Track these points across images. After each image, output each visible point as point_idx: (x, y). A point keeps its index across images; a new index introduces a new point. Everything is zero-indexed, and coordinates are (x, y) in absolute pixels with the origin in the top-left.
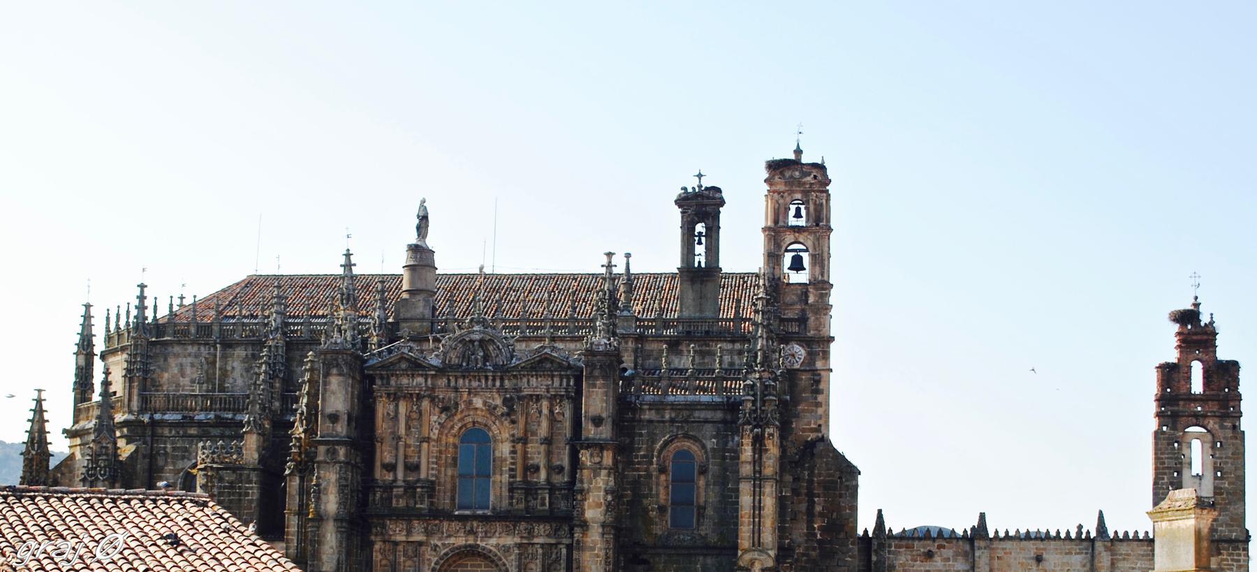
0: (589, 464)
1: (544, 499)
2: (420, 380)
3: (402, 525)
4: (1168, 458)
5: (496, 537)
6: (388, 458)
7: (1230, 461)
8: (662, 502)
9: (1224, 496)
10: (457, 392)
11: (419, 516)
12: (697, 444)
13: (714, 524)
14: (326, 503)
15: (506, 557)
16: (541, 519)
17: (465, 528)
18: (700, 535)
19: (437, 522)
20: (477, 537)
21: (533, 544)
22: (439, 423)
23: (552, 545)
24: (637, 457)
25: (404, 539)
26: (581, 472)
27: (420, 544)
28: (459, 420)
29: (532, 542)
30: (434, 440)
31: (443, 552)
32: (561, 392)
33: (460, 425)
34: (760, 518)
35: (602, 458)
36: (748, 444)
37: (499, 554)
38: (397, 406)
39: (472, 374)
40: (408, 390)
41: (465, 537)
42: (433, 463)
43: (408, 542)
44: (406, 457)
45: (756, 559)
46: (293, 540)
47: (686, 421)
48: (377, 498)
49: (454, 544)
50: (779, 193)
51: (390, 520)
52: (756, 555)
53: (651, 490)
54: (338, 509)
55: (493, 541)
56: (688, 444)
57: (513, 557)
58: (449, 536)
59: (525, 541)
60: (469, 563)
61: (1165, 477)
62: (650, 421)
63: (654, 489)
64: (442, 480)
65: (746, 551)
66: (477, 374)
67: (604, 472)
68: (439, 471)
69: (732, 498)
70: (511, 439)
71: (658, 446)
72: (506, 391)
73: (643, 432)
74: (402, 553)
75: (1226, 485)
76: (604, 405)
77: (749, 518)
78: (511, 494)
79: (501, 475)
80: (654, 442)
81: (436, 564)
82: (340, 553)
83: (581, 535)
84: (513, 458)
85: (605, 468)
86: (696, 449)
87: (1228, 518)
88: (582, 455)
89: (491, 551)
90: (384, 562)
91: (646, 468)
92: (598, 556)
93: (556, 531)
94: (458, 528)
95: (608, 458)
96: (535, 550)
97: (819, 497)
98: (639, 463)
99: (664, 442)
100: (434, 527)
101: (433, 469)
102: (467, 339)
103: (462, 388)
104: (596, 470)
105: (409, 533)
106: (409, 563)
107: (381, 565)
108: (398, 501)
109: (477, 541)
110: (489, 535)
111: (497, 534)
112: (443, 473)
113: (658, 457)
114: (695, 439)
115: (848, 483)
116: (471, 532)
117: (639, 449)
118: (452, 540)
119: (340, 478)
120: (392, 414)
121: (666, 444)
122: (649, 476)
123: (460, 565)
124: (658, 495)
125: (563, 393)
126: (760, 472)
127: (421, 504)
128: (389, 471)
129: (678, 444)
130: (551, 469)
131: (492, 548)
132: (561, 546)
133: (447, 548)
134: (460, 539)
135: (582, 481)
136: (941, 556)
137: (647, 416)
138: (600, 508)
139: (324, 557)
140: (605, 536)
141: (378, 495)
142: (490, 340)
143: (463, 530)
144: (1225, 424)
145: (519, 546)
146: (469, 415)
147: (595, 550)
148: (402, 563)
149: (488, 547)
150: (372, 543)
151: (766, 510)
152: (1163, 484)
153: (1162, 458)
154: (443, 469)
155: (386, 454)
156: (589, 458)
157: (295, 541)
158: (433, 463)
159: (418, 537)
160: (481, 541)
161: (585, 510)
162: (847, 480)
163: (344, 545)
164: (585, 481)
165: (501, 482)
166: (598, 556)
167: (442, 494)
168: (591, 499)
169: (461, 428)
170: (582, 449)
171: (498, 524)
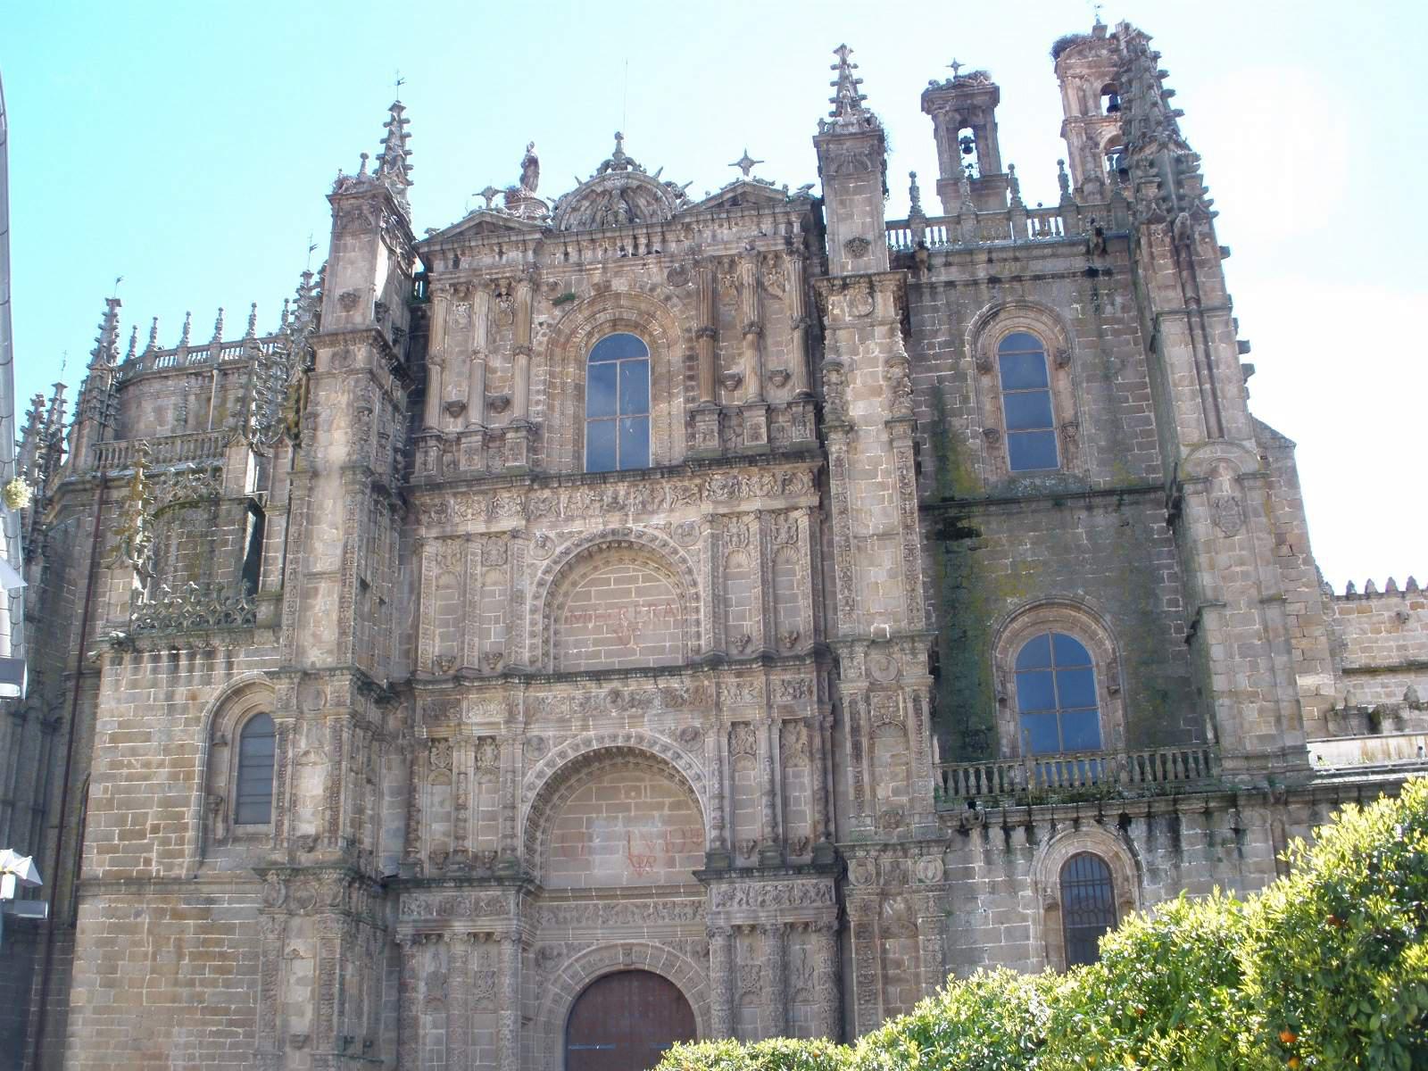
0: (848, 319)
1: (758, 426)
2: (514, 255)
3: (480, 503)
6: (453, 395)
8: (990, 423)
10: (581, 271)
11: (510, 479)
12: (1044, 318)
13: (1101, 450)
14: (326, 447)
15: (685, 547)
16: (751, 460)
17: (602, 500)
18: (1075, 477)
19: (547, 493)
20: (627, 515)
21: (739, 515)
22: (549, 326)
23: (776, 512)
24: (932, 346)
25: (482, 528)
26: (834, 334)
27: (515, 534)
28: (587, 319)
29: (738, 509)
30: (539, 354)
31: (558, 550)
32: (776, 245)
33: (588, 328)
34: (1213, 384)
35: (874, 305)
36: (1164, 257)
37: (672, 543)
38: (471, 306)
39: (609, 234)
40: (491, 274)
41: (604, 516)
42: (538, 392)
43: (489, 535)
44: (486, 388)
45: (1220, 460)
46: (276, 558)
47: (1018, 279)
48: (430, 460)
49: (581, 532)
50: (1081, 78)
51: (455, 495)
52: (1217, 451)
53: (966, 399)
54: (349, 454)
55: (659, 519)
56: (1028, 321)
57: (700, 545)
58: (570, 519)
59: (722, 510)
60: (612, 576)
62: (950, 284)
63: (972, 395)
64: (556, 422)
65: (1195, 447)
66: (617, 234)
67: (880, 331)
68: (551, 408)
69: (1127, 400)
70: (687, 335)
71: (970, 325)
72: (672, 257)
73: (939, 303)
74: (479, 558)
76: (868, 220)
77: (1192, 384)
78: (690, 430)
81: (546, 572)
82: (348, 533)
83: (844, 448)
84: (690, 368)
85: (882, 323)
86: (1043, 327)
88: (833, 305)
89: (654, 539)
90: (443, 580)
91: (952, 364)
92: (883, 486)
93: (786, 482)
94: (588, 502)
95: (885, 306)
96: (743, 528)
98: (935, 357)
99: (980, 317)
100: (542, 506)
101: (538, 402)
102: (599, 190)
103: (591, 264)
104: (866, 323)
105: (491, 515)
106: (494, 576)
108: (470, 460)
109: (626, 521)
110: (649, 508)
112: (557, 410)
113: (974, 342)
114: (1039, 308)
115: (1279, 465)
116: (616, 505)
117: (935, 333)
118: (577, 526)
119: (357, 399)
120: (463, 321)
121: (984, 323)
122: (960, 376)
123: (593, 582)
124: (980, 409)
125: (780, 247)
126: (1198, 301)
127: (516, 460)
128: (455, 415)
129: (1008, 322)
130: (765, 378)
131: (656, 533)
132: (795, 514)
134: (593, 520)
135: (837, 351)
136: (1419, 620)
137: (942, 276)
138: (880, 395)
139: (319, 546)
140: (895, 444)
141: (433, 453)
142: (638, 187)
143: (597, 505)
145: (713, 519)
146: (605, 309)
147: (876, 477)
148: (479, 577)
149: (649, 531)
150: (419, 545)
151: (1222, 367)
154: (557, 403)
155: (450, 388)
156: (846, 309)
157: (280, 560)
158: (538, 392)
159: (507, 523)
160: (635, 521)
161: (847, 402)
162: (1277, 460)
163: (357, 517)
164: (843, 350)
166: (883, 486)
167: (556, 446)
168: (859, 381)
169: (590, 335)
170: (831, 290)
171: (667, 486)
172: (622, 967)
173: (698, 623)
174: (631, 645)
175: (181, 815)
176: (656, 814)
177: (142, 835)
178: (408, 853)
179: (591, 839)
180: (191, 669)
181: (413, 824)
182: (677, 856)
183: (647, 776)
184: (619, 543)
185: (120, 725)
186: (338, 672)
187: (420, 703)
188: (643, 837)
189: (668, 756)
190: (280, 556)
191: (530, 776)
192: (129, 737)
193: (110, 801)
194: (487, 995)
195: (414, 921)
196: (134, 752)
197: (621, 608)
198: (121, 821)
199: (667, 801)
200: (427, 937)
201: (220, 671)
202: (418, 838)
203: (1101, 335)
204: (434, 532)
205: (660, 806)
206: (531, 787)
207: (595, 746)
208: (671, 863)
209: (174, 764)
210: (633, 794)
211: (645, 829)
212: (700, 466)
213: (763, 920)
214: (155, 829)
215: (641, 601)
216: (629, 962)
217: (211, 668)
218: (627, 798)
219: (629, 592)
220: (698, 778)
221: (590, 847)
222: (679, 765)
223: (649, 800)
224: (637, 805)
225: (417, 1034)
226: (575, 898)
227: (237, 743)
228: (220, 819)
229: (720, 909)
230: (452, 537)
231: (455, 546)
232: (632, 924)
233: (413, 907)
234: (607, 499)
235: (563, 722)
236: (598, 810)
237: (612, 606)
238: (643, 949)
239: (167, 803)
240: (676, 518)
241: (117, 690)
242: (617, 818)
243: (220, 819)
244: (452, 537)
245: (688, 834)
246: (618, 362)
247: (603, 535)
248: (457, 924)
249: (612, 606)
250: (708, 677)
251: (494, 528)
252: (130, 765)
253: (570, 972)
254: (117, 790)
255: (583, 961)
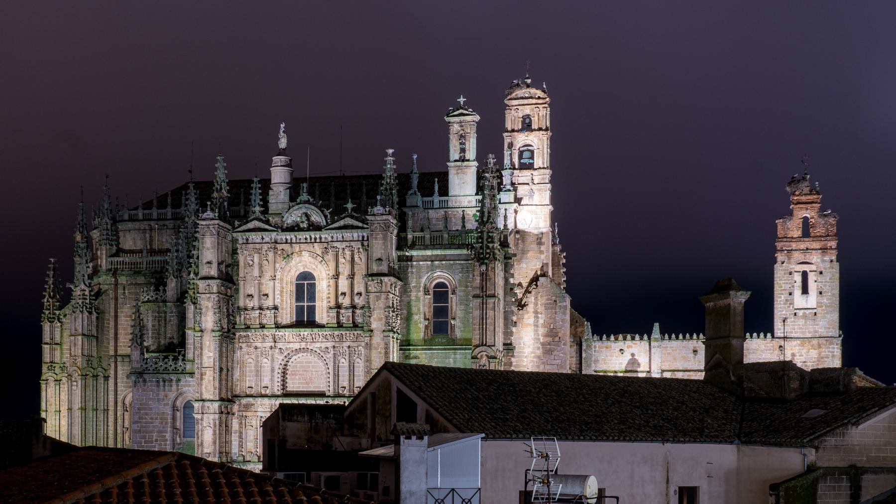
4: (784, 283)
7: (828, 284)
9: (824, 308)
61: (783, 296)
75: (825, 300)
80: (420, 277)
87: (826, 323)
97: (541, 314)
144: (825, 258)
152: (780, 301)
153: (780, 284)
166: (380, 353)
174: (310, 385)
175: (165, 436)
177: (152, 442)
180: (164, 386)
185: (141, 404)
190: (192, 347)
192: (144, 409)
193: (140, 431)
196: (147, 414)
198: (144, 437)
201: (174, 387)
203: (467, 287)
209: (161, 419)
214: (156, 440)
215: (313, 370)
217: (171, 386)
227: (182, 410)
228: (178, 436)
239: (159, 432)
240: (323, 345)
241: (138, 392)
243: (178, 436)
246: (306, 282)
252: (146, 418)
254: (142, 427)
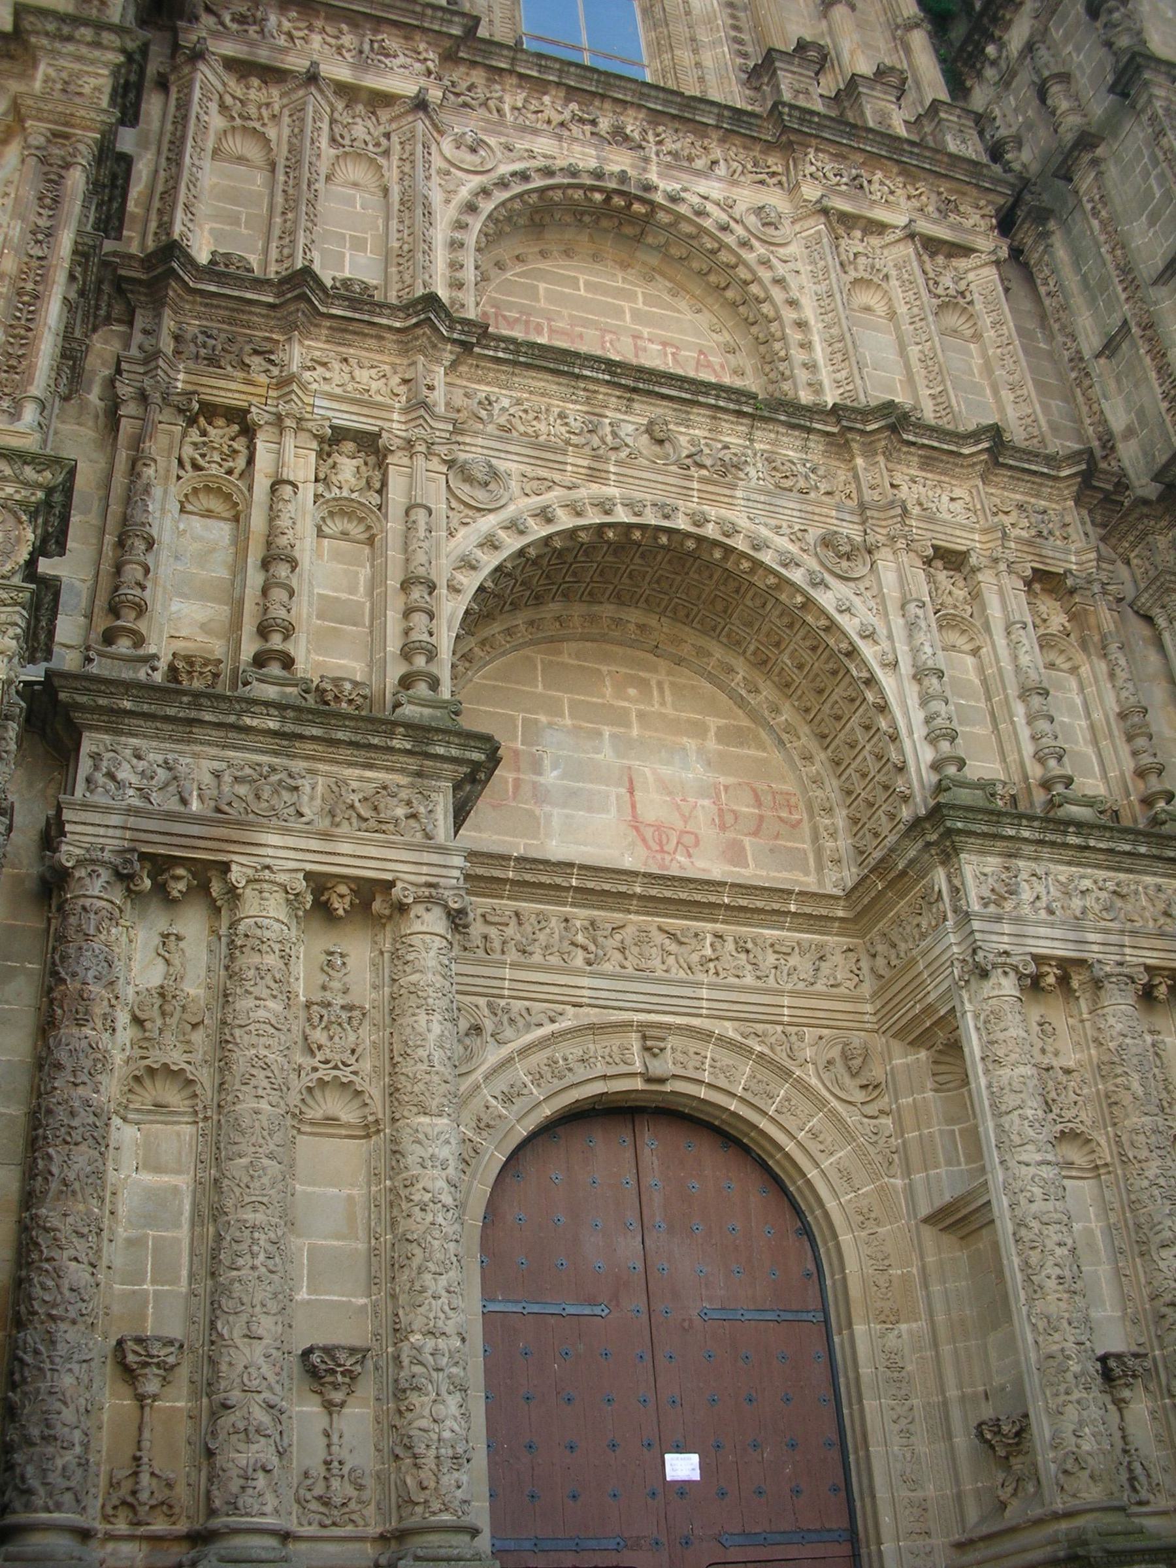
5: (720, 179)
17: (594, 123)
19: (478, 76)
20: (646, 160)
23: (931, 246)
27: (420, 104)
29: (869, 215)
31: (505, 169)
55: (713, 188)
57: (793, 249)
60: (582, 279)
79: (695, 51)
94: (567, 115)
107: (216, 152)
109: (645, 170)
111: (721, 170)
132: (962, 263)
133: (521, 159)
134: (577, 148)
160: (660, 175)
165: (698, 65)
172: (639, 1084)
173: (811, 367)
176: (691, 744)
178: (109, 637)
179: (536, 766)
181: (132, 572)
182: (747, 841)
183: (663, 664)
184: (630, 198)
186: (86, 33)
187: (169, 323)
188: (665, 787)
189: (797, 576)
191: (466, 540)
194: (345, 1075)
195: (131, 811)
197: (604, 331)
199: (713, 722)
200: (160, 865)
202: (141, 609)
204: (229, 48)
205: (699, 731)
206: (469, 564)
207: (622, 515)
208: (735, 853)
210: (632, 692)
211: (666, 771)
212: (802, 121)
213: (1093, 953)
215: (646, 332)
216: (658, 1067)
218: (620, 693)
219: (619, 313)
220: (869, 635)
221: (535, 785)
222: (826, 600)
223: (669, 711)
224: (641, 715)
225: (99, 1175)
226: (522, 888)
229: (992, 909)
230: (272, 74)
231: (256, 92)
232: (659, 973)
233: (124, 774)
234: (604, 125)
235: (543, 450)
236: (554, 709)
237: (586, 323)
238: (693, 1046)
242: (600, 734)
244: (272, 74)
245: (767, 799)
247: (598, 174)
248: (273, 839)
249: (586, 323)
250: (869, 452)
251: (372, 81)
253: (501, 1084)
255: (538, 1058)
